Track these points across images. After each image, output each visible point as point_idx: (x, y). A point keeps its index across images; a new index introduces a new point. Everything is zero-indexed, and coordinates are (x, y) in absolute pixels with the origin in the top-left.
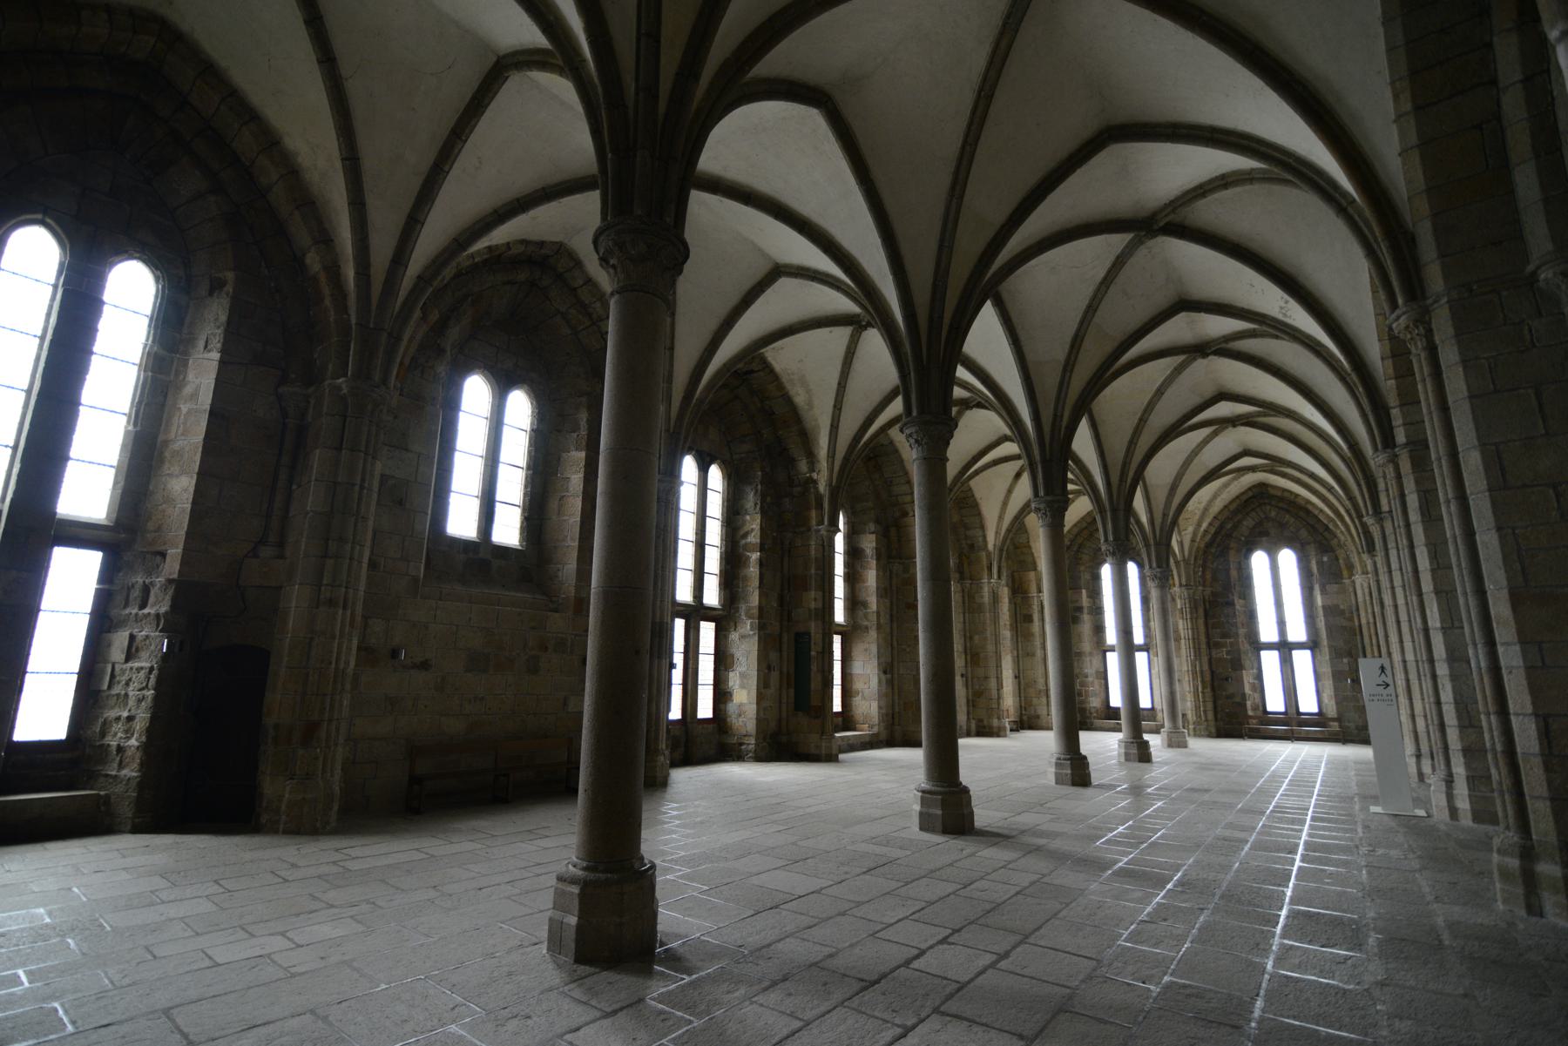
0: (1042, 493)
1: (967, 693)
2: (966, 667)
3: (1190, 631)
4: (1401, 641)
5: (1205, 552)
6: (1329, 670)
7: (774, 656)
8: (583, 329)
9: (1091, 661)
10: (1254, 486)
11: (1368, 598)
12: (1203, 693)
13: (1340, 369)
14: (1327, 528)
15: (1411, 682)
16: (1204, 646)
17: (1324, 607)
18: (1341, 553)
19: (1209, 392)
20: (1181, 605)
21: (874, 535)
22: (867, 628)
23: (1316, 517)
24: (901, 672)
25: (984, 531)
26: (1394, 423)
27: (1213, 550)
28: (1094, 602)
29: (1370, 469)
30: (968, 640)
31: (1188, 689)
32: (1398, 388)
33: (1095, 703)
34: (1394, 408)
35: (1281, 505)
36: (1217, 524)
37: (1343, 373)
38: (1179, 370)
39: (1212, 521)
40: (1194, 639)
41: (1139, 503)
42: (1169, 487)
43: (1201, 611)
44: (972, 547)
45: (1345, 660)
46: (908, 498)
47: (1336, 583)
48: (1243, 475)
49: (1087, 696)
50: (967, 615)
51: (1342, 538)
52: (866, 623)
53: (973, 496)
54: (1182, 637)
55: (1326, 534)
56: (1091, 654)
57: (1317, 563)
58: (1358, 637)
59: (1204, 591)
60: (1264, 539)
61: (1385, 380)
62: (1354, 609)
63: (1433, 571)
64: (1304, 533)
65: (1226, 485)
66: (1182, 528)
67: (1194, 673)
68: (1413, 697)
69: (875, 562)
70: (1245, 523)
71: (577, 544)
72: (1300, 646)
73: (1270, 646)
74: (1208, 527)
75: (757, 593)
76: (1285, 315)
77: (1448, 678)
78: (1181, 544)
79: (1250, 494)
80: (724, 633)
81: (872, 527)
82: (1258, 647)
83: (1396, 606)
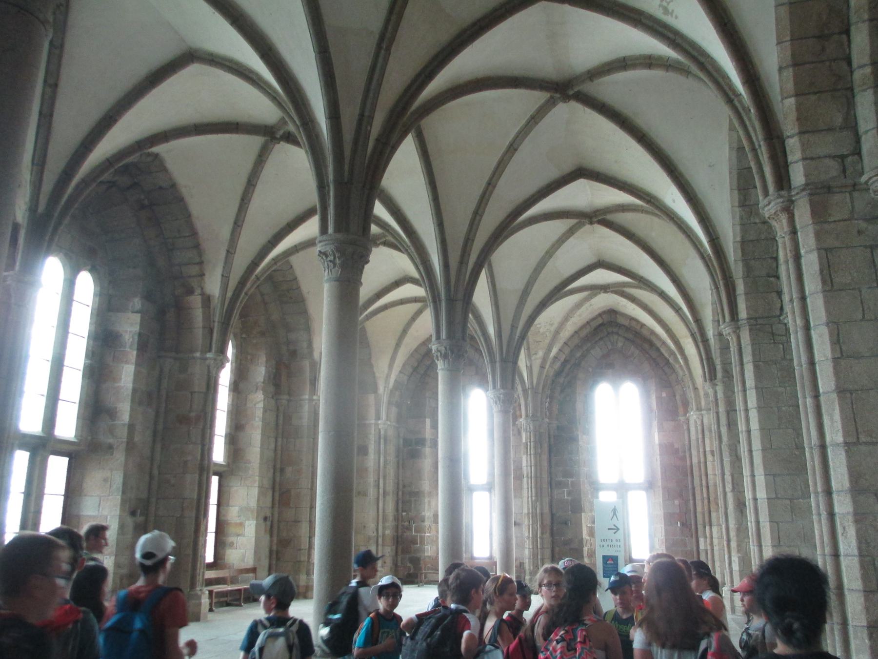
0: (331, 229)
1: (271, 541)
2: (273, 507)
4: (753, 476)
5: (553, 381)
9: (429, 502)
10: (604, 313)
11: (700, 436)
12: (542, 538)
13: (726, 88)
14: (667, 362)
15: (761, 524)
16: (546, 486)
17: (660, 445)
20: (526, 440)
21: (139, 315)
22: (110, 447)
23: (658, 350)
25: (310, 336)
26: (790, 158)
27: (561, 380)
29: (729, 268)
30: (278, 474)
31: (526, 535)
32: (798, 109)
34: (792, 137)
36: (567, 350)
37: (730, 94)
39: (563, 347)
40: (536, 477)
41: (481, 296)
42: (520, 293)
43: (546, 446)
44: (294, 354)
48: (595, 295)
49: (422, 543)
50: (280, 440)
51: (681, 373)
52: (111, 440)
53: (299, 288)
54: (525, 475)
58: (689, 478)
59: (549, 424)
61: (782, 99)
62: (687, 448)
63: (836, 361)
65: (579, 305)
66: (532, 352)
67: (534, 515)
68: (763, 544)
69: (135, 353)
70: (592, 352)
74: (558, 353)
76: (666, 11)
77: (850, 518)
78: (530, 369)
79: (600, 321)
81: (137, 303)
83: (749, 432)
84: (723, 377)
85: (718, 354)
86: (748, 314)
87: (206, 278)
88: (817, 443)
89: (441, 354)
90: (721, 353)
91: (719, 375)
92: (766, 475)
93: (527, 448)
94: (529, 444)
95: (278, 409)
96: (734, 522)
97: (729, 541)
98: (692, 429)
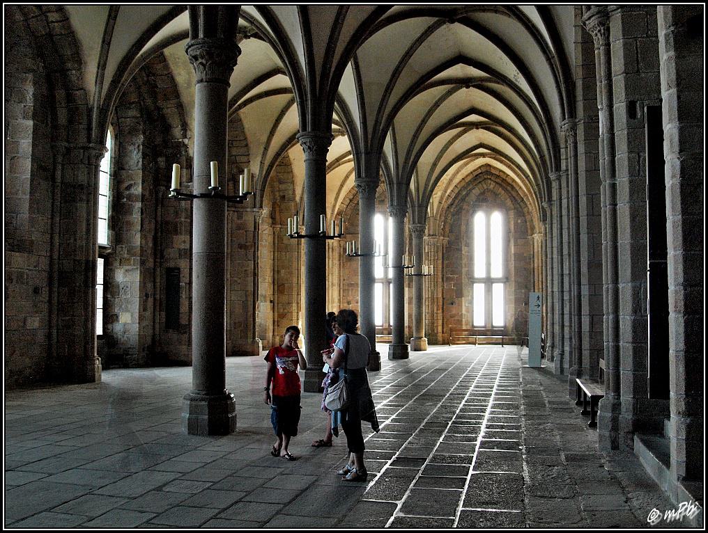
7: (149, 285)
8: (33, 17)
11: (540, 250)
16: (440, 280)
17: (515, 254)
18: (528, 218)
19: (465, 107)
24: (232, 299)
30: (276, 273)
35: (498, 180)
36: (457, 191)
38: (450, 93)
43: (440, 254)
44: (283, 197)
45: (523, 291)
46: (244, 159)
51: (530, 208)
58: (532, 277)
60: (484, 204)
64: (509, 202)
70: (473, 191)
71: (28, 196)
72: (498, 280)
73: (480, 281)
75: (138, 235)
80: (110, 267)
82: (472, 280)
83: (552, 258)
87: (251, 162)
91: (548, 219)
95: (274, 233)
98: (536, 244)
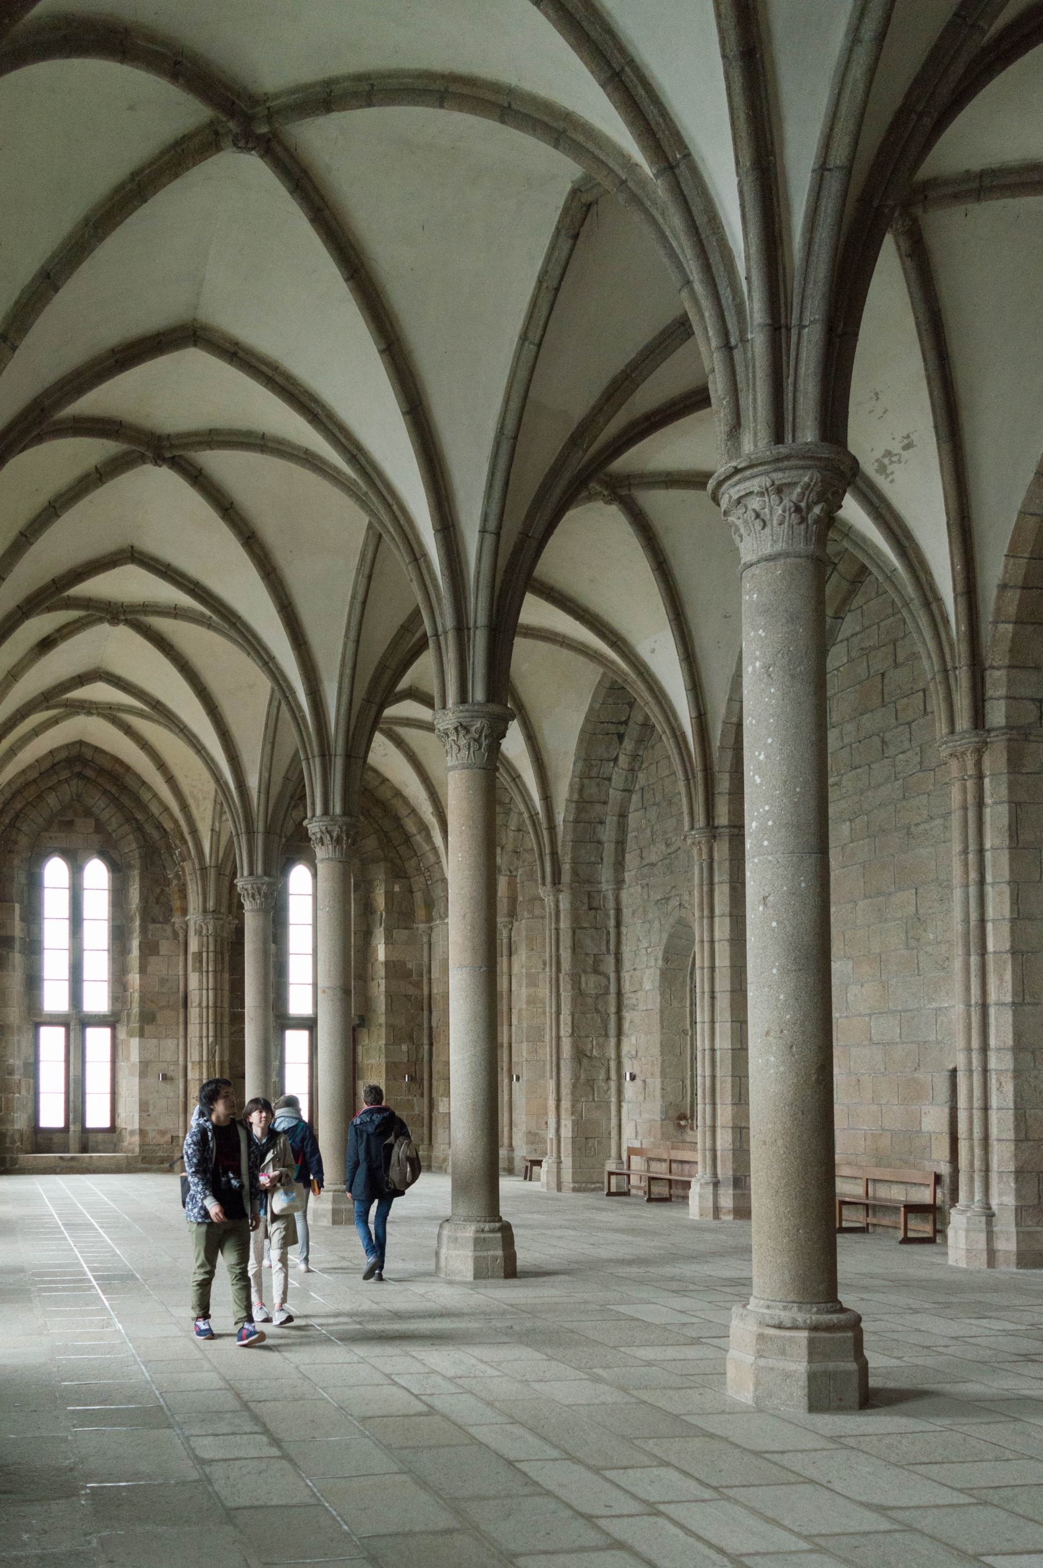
3: (211, 993)
6: (383, 1060)
14: (407, 839)
17: (387, 963)
18: (418, 883)
20: (201, 945)
23: (397, 820)
28: (29, 930)
33: (20, 1122)
40: (215, 1007)
45: (404, 1047)
47: (406, 928)
51: (432, 859)
55: (402, 849)
56: (19, 1028)
57: (386, 893)
58: (426, 1013)
84: (572, 882)
85: (569, 849)
86: (729, 820)
88: (980, 1002)
89: (332, 837)
90: (573, 847)
91: (566, 877)
92: (732, 1021)
93: (201, 962)
94: (205, 954)
96: (569, 1076)
97: (558, 1100)
